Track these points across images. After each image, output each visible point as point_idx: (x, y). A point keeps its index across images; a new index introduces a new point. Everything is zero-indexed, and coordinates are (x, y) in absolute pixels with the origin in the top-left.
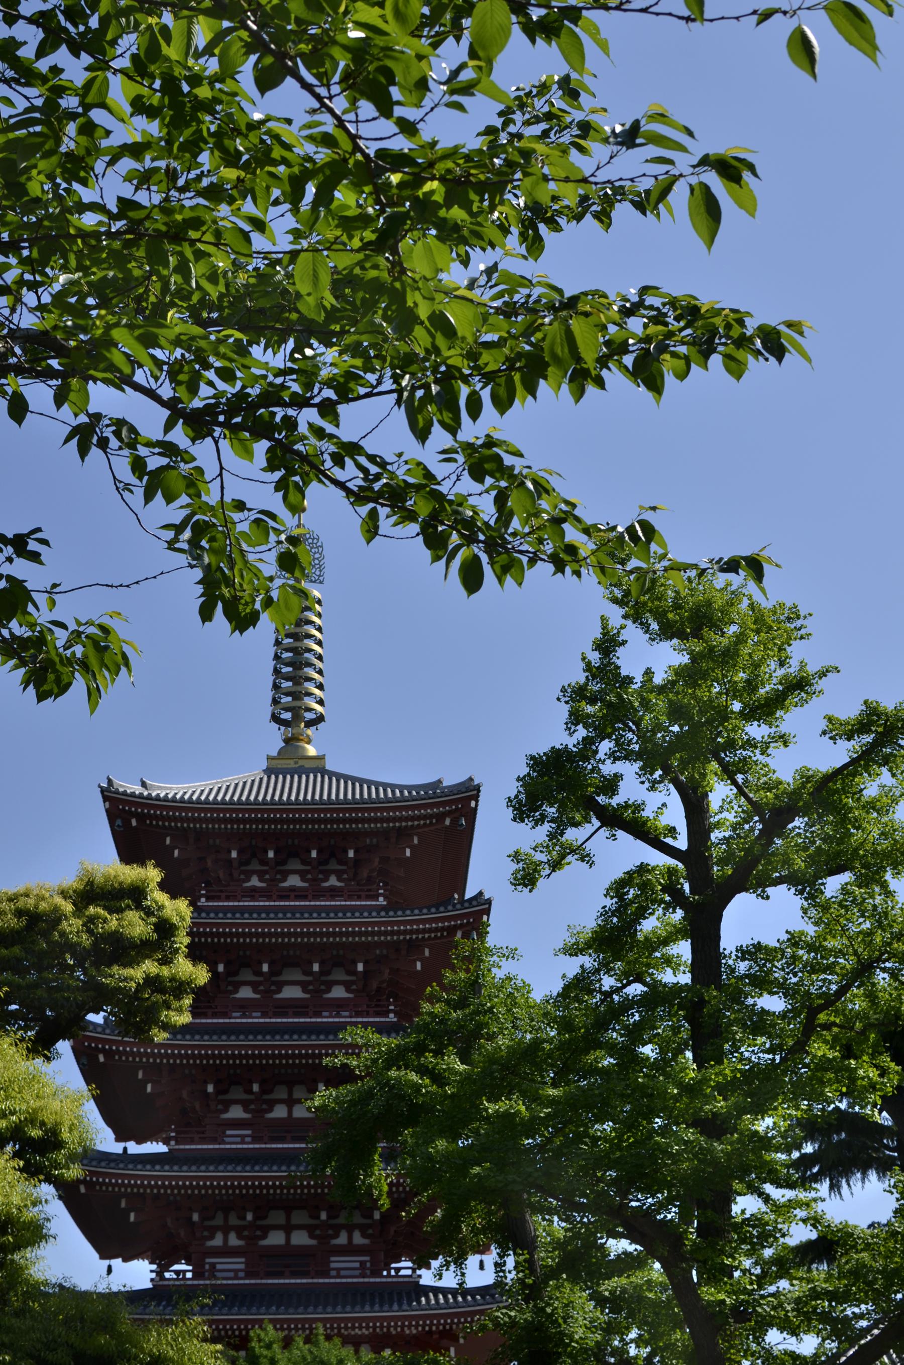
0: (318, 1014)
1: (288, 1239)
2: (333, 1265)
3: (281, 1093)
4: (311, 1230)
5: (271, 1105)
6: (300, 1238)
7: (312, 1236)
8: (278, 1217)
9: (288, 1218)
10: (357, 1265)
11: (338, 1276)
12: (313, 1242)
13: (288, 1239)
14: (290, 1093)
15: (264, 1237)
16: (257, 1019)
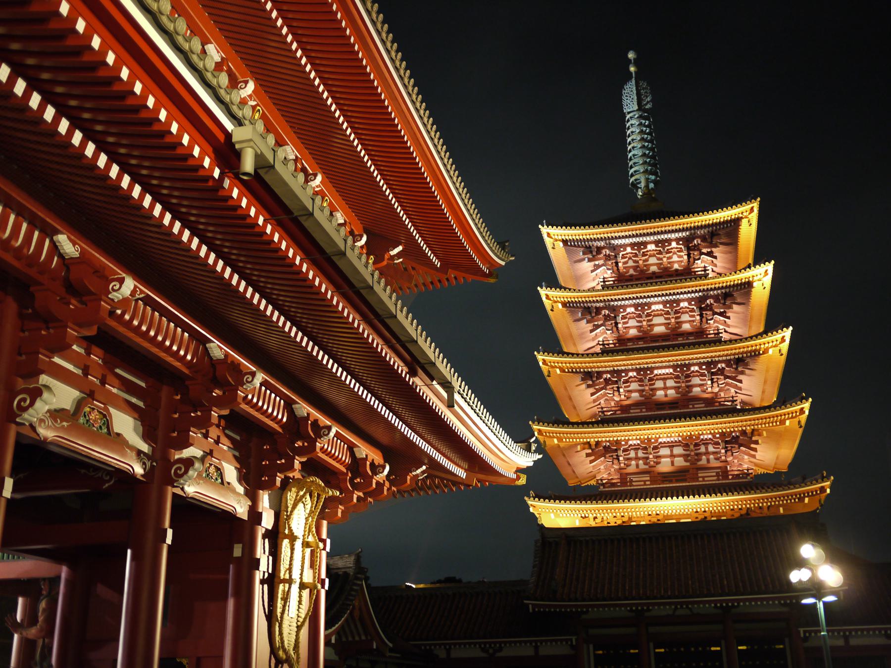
6: (680, 462)
7: (686, 461)
8: (665, 451)
9: (672, 451)
11: (704, 481)
14: (665, 384)
16: (641, 344)
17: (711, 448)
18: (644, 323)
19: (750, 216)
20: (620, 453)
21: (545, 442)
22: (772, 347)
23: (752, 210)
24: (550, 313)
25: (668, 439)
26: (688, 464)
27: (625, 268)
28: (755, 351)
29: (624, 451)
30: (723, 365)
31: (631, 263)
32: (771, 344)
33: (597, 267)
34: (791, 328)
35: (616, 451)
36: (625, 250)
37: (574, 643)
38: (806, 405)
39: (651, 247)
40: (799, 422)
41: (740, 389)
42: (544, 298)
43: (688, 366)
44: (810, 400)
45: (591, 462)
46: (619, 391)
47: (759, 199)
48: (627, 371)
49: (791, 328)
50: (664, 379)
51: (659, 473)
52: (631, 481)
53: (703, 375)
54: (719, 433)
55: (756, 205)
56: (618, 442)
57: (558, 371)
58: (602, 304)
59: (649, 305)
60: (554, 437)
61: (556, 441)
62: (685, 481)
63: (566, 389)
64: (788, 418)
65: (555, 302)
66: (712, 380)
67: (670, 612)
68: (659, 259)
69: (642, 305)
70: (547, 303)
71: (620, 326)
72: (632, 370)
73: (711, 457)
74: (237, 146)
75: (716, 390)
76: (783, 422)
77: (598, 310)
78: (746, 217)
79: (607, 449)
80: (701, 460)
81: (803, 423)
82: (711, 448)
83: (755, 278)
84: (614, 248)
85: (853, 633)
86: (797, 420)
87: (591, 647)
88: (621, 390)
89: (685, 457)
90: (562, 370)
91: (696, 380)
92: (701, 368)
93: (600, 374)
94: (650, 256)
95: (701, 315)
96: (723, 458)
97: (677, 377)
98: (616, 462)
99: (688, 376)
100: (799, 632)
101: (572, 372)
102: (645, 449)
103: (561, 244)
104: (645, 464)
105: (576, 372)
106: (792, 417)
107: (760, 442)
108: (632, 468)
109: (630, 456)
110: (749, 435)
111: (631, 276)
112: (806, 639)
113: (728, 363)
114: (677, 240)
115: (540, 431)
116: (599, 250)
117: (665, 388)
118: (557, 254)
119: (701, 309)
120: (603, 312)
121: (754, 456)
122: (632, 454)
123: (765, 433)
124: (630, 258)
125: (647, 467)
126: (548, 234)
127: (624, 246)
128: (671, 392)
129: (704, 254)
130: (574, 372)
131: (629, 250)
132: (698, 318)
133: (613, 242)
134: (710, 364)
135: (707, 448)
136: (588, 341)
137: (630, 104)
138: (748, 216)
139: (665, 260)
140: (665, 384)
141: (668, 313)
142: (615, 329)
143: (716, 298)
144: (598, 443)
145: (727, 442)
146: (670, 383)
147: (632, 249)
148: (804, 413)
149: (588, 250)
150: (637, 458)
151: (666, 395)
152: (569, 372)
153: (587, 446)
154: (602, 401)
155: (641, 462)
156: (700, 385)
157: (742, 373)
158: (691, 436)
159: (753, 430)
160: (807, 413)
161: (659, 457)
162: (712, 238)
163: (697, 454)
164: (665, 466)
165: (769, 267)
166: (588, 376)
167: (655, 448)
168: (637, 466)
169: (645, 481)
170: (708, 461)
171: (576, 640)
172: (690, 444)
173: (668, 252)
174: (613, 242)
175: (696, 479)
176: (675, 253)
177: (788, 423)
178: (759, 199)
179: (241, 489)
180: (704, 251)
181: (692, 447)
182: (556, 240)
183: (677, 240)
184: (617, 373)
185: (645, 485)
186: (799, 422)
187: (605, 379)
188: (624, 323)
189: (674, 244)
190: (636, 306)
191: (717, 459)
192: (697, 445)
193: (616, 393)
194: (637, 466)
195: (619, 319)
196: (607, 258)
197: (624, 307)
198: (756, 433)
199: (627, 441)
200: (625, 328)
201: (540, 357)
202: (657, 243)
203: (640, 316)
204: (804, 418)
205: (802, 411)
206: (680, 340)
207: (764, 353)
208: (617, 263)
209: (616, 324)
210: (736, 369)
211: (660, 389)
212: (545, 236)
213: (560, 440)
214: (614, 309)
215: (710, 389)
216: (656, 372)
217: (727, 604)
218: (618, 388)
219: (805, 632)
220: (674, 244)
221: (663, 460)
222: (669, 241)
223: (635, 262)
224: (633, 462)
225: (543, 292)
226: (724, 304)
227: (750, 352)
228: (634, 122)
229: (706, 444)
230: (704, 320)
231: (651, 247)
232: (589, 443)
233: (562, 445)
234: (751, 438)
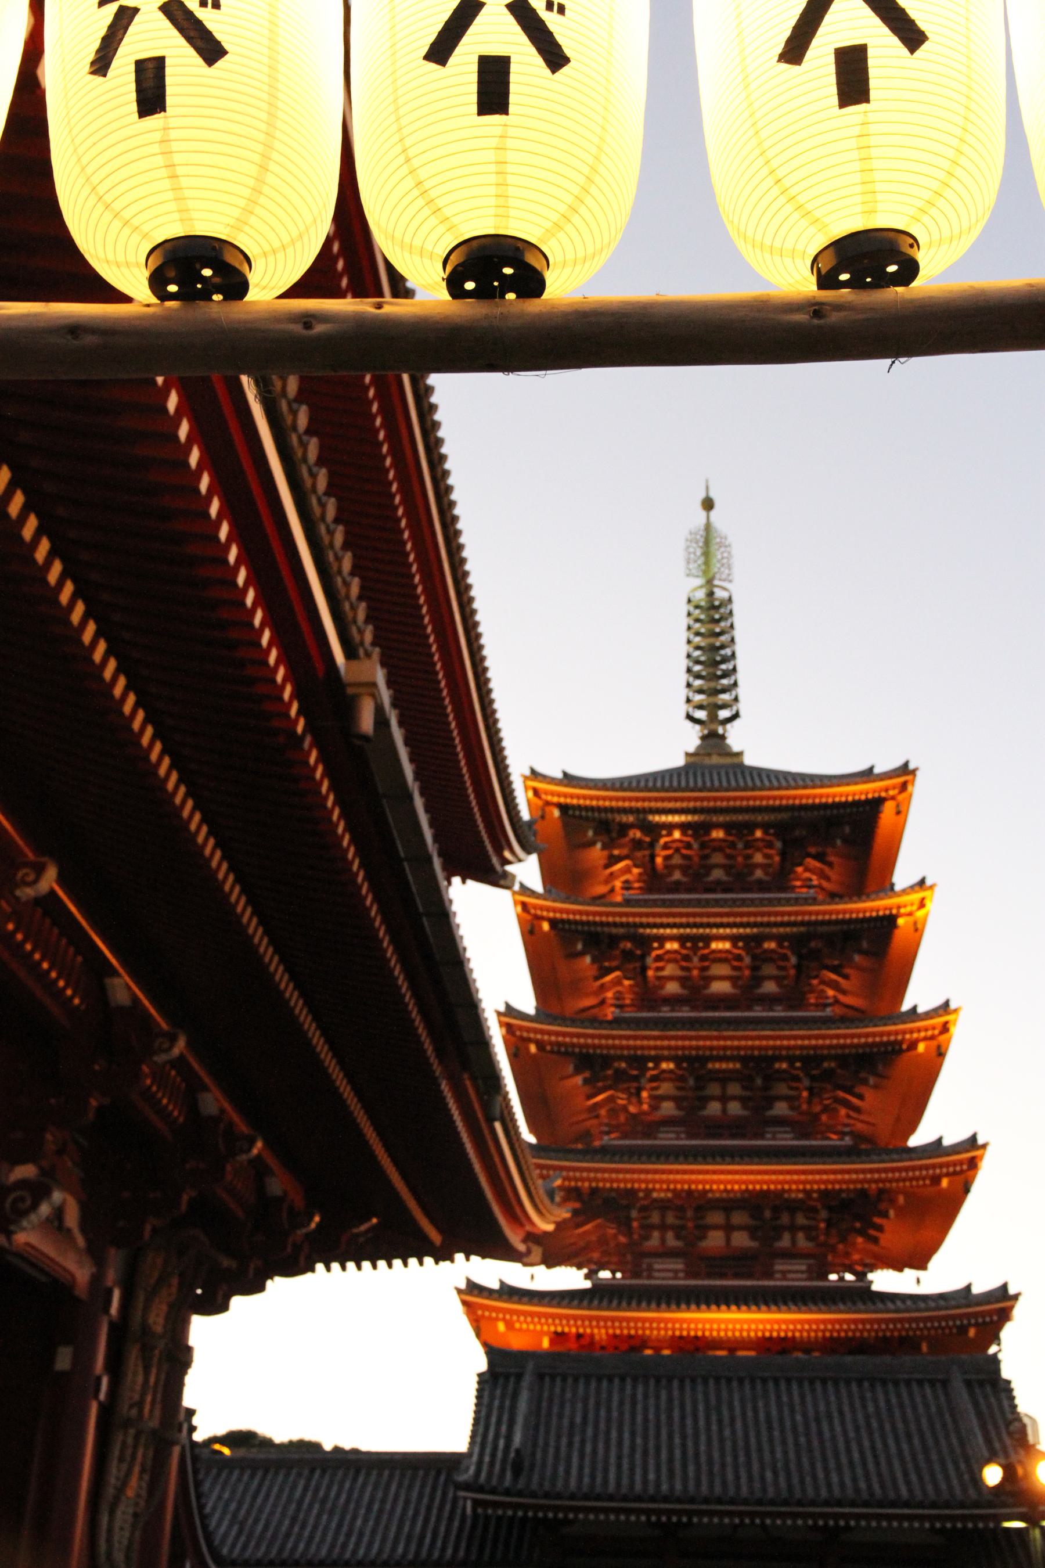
0: (749, 1008)
1: (728, 1240)
2: (778, 1267)
3: (714, 1089)
4: (752, 1232)
5: (705, 1100)
6: (741, 1240)
7: (753, 1237)
8: (716, 1218)
9: (728, 1218)
10: (804, 1268)
11: (785, 1279)
12: (754, 1244)
13: (728, 1240)
15: (704, 1237)
16: (685, 1013)
18: (695, 973)
19: (900, 797)
22: (925, 1039)
27: (666, 867)
29: (643, 1209)
30: (833, 1065)
31: (677, 860)
32: (923, 1034)
33: (613, 860)
36: (670, 834)
41: (857, 1110)
45: (579, 1225)
46: (638, 1094)
52: (650, 1269)
53: (796, 1079)
54: (819, 1191)
56: (633, 1192)
57: (533, 1048)
58: (621, 931)
59: (708, 939)
62: (749, 1276)
66: (811, 1090)
68: (729, 857)
69: (694, 939)
71: (650, 973)
72: (667, 1059)
74: (350, 691)
75: (817, 1109)
76: (936, 1180)
77: (614, 940)
78: (893, 798)
80: (779, 1238)
82: (801, 1220)
83: (903, 911)
84: (654, 831)
88: (645, 1094)
90: (540, 1045)
93: (607, 1061)
94: (715, 850)
96: (822, 1238)
101: (559, 1052)
103: (556, 813)
105: (567, 1053)
107: (892, 1213)
109: (649, 1221)
111: (678, 883)
114: (765, 827)
116: (624, 828)
117: (724, 1099)
120: (622, 945)
121: (875, 1240)
122: (655, 1218)
123: (901, 1199)
124: (677, 850)
128: (735, 1108)
129: (809, 855)
131: (677, 835)
133: (650, 818)
134: (811, 1060)
136: (587, 995)
139: (740, 859)
141: (739, 958)
144: (594, 1191)
145: (830, 1209)
146: (734, 1089)
147: (684, 833)
154: (603, 1112)
155: (670, 1235)
157: (865, 1082)
158: (765, 1194)
159: (881, 1191)
168: (663, 1240)
169: (676, 1272)
173: (748, 845)
174: (650, 818)
175: (769, 1275)
176: (758, 849)
177: (945, 1183)
179: (81, 1241)
180: (813, 850)
181: (768, 1214)
184: (639, 1061)
185: (676, 1278)
187: (617, 1071)
188: (658, 969)
189: (759, 834)
190: (682, 939)
191: (809, 1238)
192: (776, 1210)
193: (634, 1100)
194: (663, 1240)
195: (649, 960)
196: (637, 844)
197: (662, 940)
199: (648, 1192)
200: (659, 978)
202: (727, 827)
203: (687, 958)
206: (758, 1013)
208: (653, 857)
209: (644, 969)
211: (713, 1098)
214: (645, 943)
215: (805, 1107)
217: (836, 1523)
218: (639, 1090)
222: (751, 827)
223: (685, 857)
232: (577, 1190)
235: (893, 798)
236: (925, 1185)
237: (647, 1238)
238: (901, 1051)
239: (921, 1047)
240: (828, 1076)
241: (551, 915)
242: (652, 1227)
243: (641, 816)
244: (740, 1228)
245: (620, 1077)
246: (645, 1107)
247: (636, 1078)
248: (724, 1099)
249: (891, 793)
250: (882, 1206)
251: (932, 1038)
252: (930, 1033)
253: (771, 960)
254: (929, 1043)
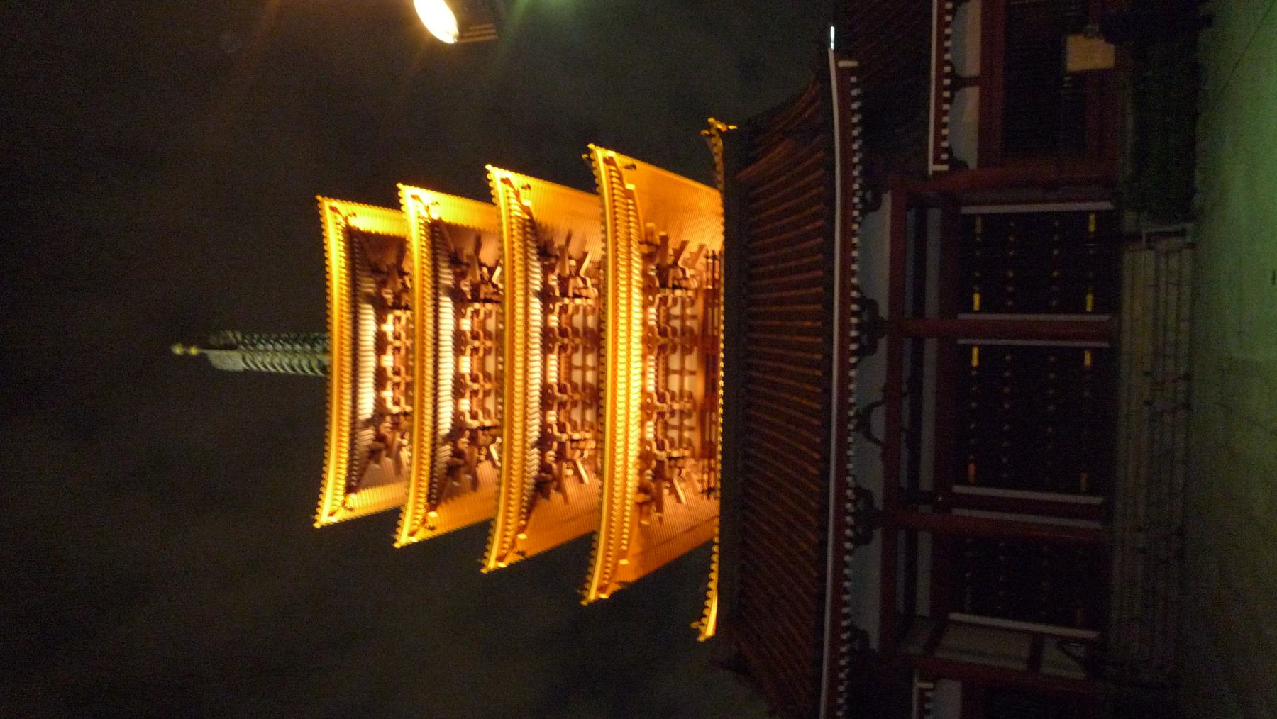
6: (692, 362)
7: (690, 352)
14: (577, 368)
15: (691, 396)
17: (676, 311)
20: (663, 455)
21: (620, 583)
23: (333, 209)
24: (439, 531)
25: (652, 376)
26: (696, 349)
28: (524, 227)
29: (661, 447)
32: (513, 200)
34: (489, 167)
35: (660, 463)
37: (930, 685)
38: (600, 154)
39: (388, 361)
40: (627, 167)
42: (414, 540)
43: (546, 332)
44: (591, 146)
47: (319, 198)
48: (544, 426)
49: (489, 167)
50: (570, 367)
51: (706, 396)
53: (564, 309)
55: (327, 204)
56: (645, 457)
57: (522, 536)
60: (616, 565)
61: (624, 562)
63: (573, 519)
64: (622, 184)
65: (424, 521)
67: (879, 450)
70: (423, 534)
71: (488, 423)
73: (689, 311)
76: (629, 194)
78: (346, 219)
79: (659, 475)
80: (691, 330)
81: (629, 161)
85: (948, 57)
86: (624, 171)
87: (955, 616)
89: (686, 351)
90: (522, 529)
91: (577, 320)
92: (552, 312)
93: (544, 467)
95: (486, 301)
96: (690, 293)
97: (563, 348)
98: (680, 463)
99: (563, 333)
100: (935, 172)
102: (661, 414)
104: (689, 415)
106: (620, 178)
107: (663, 234)
108: (694, 437)
110: (653, 249)
112: (957, 165)
113: (547, 270)
114: (380, 320)
115: (602, 589)
117: (584, 368)
118: (366, 502)
119: (476, 299)
122: (674, 434)
123: (650, 225)
125: (695, 414)
126: (332, 514)
127: (380, 402)
130: (529, 508)
131: (388, 394)
132: (489, 306)
134: (546, 296)
135: (676, 317)
137: (232, 361)
138: (341, 217)
140: (577, 368)
141: (475, 350)
142: (493, 432)
143: (460, 276)
145: (664, 285)
146: (577, 359)
148: (611, 158)
149: (374, 454)
150: (680, 428)
151: (593, 369)
152: (527, 519)
153: (645, 508)
155: (687, 422)
156: (585, 315)
157: (563, 250)
158: (646, 341)
160: (611, 154)
161: (682, 391)
162: (382, 273)
163: (683, 333)
164: (695, 385)
165: (407, 192)
166: (545, 484)
167: (662, 398)
170: (694, 317)
171: (922, 680)
172: (660, 342)
177: (630, 186)
178: (319, 198)
182: (344, 503)
183: (380, 320)
184: (544, 441)
186: (627, 167)
191: (693, 303)
193: (582, 444)
194: (691, 429)
197: (457, 415)
198: (649, 239)
199: (643, 441)
201: (492, 564)
204: (621, 160)
205: (609, 161)
207: (529, 213)
209: (484, 428)
210: (557, 257)
212: (334, 519)
213: (623, 555)
215: (590, 302)
216: (553, 380)
219: (937, 160)
220: (388, 328)
221: (687, 387)
224: (686, 434)
225: (403, 539)
226: (468, 265)
227: (525, 233)
228: (259, 359)
229: (669, 317)
230: (495, 298)
231: (388, 361)
232: (640, 505)
233: (636, 549)
234: (657, 247)
235: (346, 219)
236: (634, 205)
237: (690, 444)
238: (531, 220)
239: (527, 203)
240: (563, 282)
241: (422, 511)
242: (681, 439)
243: (359, 425)
244: (683, 361)
245: (561, 456)
246: (588, 435)
247: (562, 445)
248: (584, 368)
249: (340, 219)
250: (659, 242)
251: (517, 194)
252: (512, 195)
253: (483, 323)
254: (522, 198)
